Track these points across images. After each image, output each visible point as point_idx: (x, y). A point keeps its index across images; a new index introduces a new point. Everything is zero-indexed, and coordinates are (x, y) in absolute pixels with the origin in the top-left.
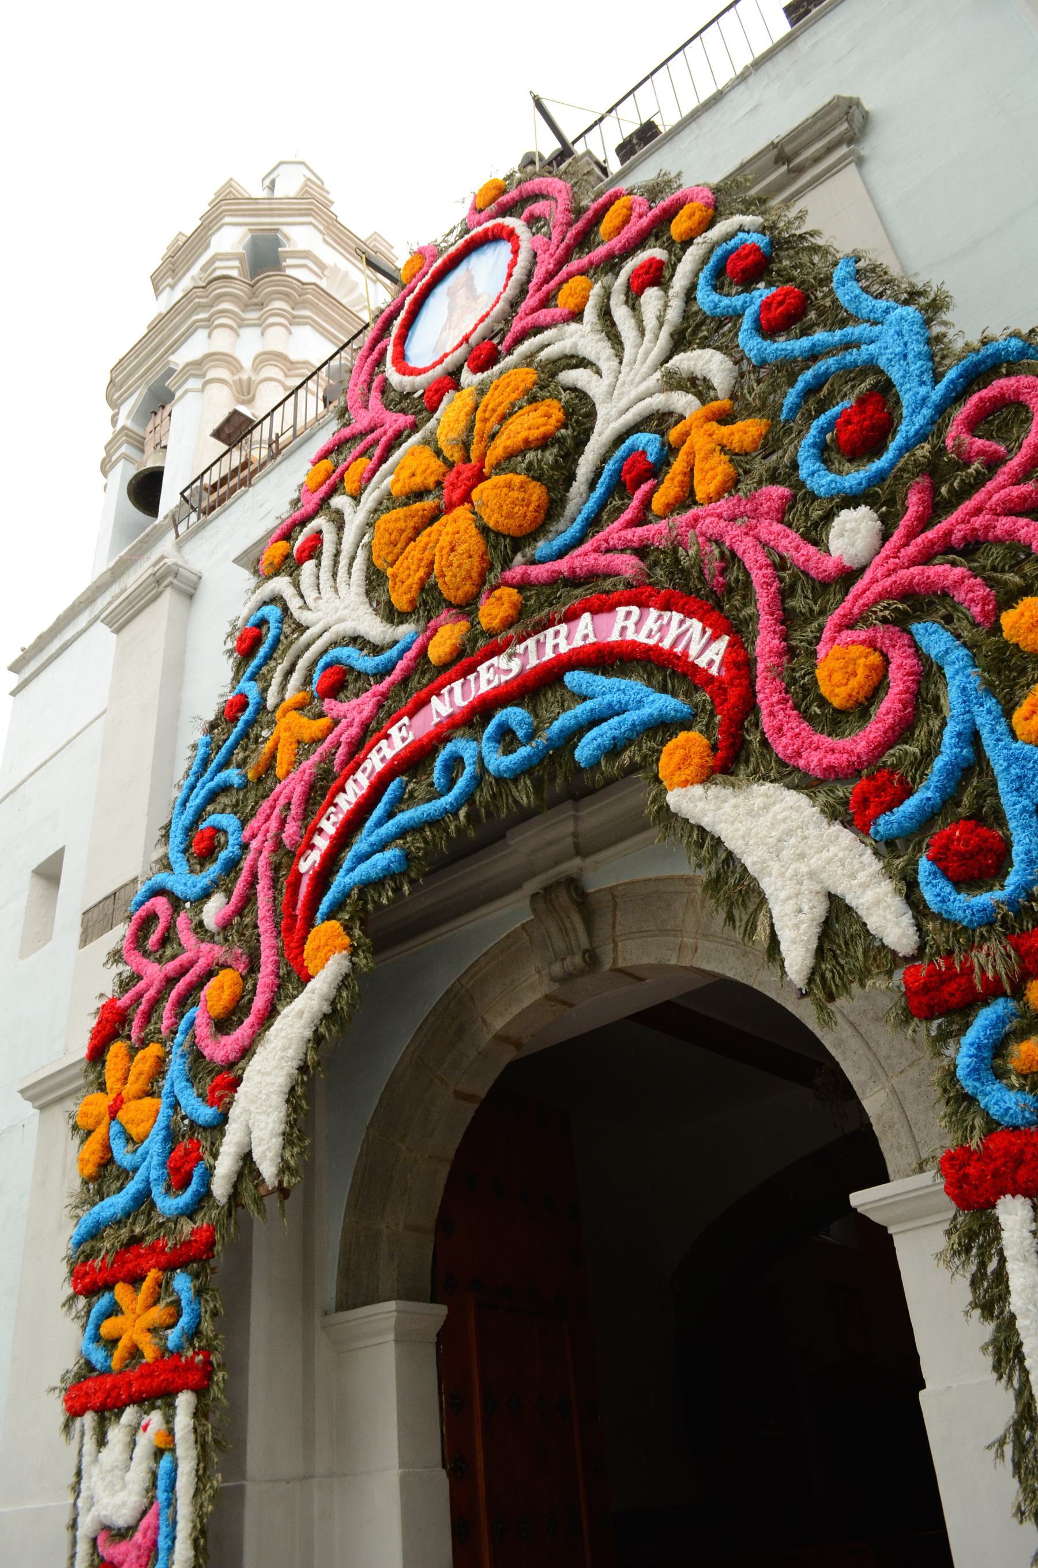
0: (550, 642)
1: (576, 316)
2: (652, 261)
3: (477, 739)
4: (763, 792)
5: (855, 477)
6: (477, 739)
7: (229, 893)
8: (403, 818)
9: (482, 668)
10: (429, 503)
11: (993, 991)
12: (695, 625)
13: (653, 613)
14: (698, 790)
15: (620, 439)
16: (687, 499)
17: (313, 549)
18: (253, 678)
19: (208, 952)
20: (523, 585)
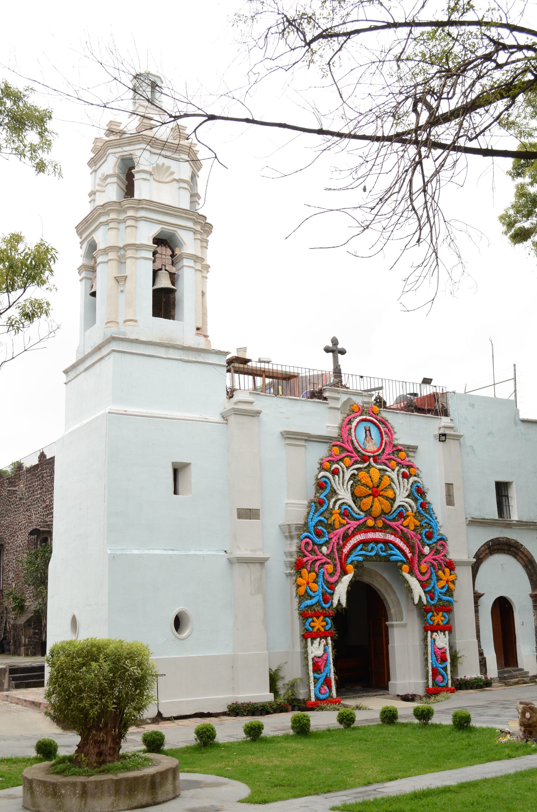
0: (388, 536)
1: (393, 470)
2: (407, 474)
3: (376, 546)
4: (415, 579)
5: (428, 542)
6: (376, 546)
7: (328, 548)
8: (364, 552)
9: (377, 533)
10: (370, 492)
11: (433, 612)
12: (408, 549)
13: (402, 543)
14: (407, 574)
15: (399, 506)
16: (407, 527)
17: (335, 472)
18: (325, 496)
19: (325, 559)
20: (383, 522)
